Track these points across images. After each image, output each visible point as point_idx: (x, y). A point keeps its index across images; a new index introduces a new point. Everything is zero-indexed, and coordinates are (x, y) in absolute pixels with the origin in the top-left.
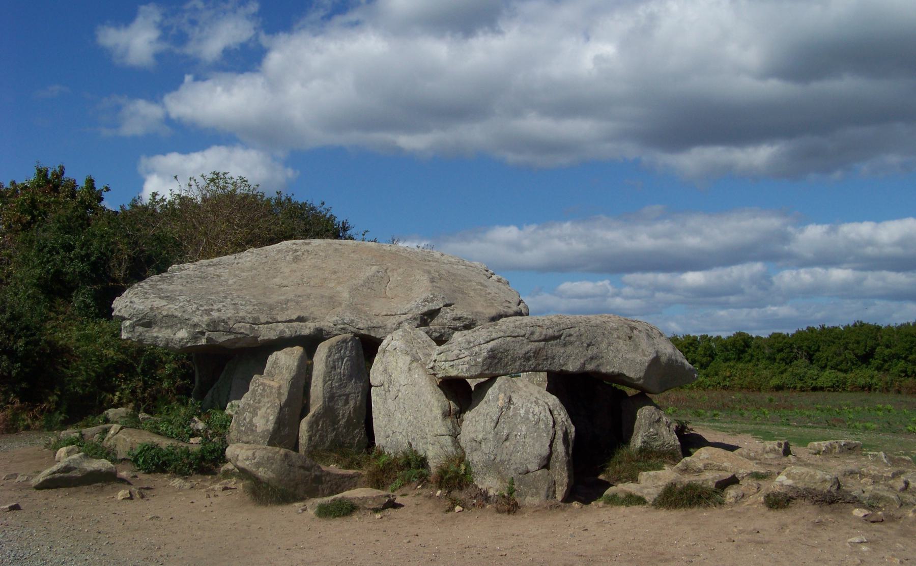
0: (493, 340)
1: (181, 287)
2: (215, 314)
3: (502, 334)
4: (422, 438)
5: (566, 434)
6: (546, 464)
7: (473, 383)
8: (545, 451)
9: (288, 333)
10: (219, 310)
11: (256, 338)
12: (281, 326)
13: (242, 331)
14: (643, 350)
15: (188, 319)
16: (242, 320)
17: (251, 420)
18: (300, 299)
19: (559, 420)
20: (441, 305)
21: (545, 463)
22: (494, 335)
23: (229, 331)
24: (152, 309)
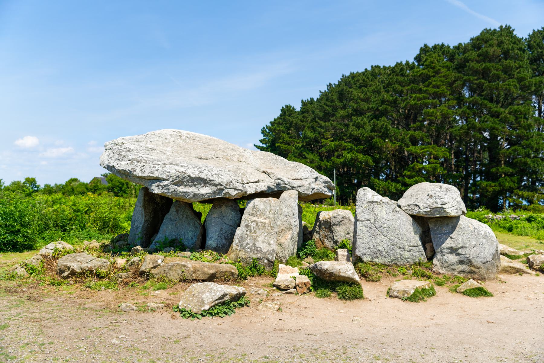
4: (400, 248)
11: (246, 192)
12: (254, 185)
13: (240, 188)
15: (213, 181)
17: (254, 244)
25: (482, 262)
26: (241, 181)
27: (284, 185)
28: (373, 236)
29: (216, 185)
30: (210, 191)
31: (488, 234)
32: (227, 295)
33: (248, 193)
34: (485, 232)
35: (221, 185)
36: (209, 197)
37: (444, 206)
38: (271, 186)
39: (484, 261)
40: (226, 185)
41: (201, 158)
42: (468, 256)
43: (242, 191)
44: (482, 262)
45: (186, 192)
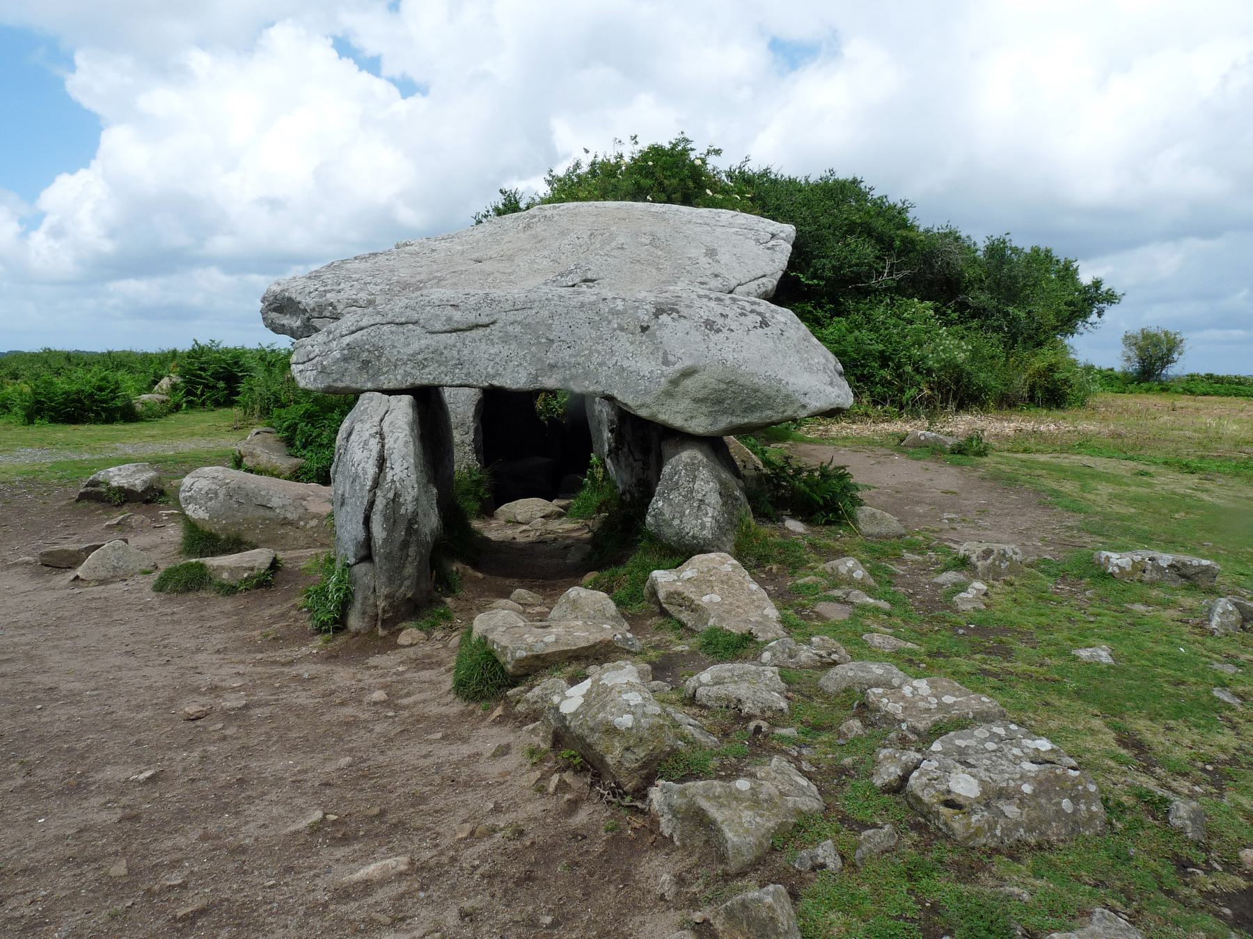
0: (362, 329)
3: (378, 319)
14: (665, 353)
21: (363, 553)
22: (363, 324)
40: (313, 310)
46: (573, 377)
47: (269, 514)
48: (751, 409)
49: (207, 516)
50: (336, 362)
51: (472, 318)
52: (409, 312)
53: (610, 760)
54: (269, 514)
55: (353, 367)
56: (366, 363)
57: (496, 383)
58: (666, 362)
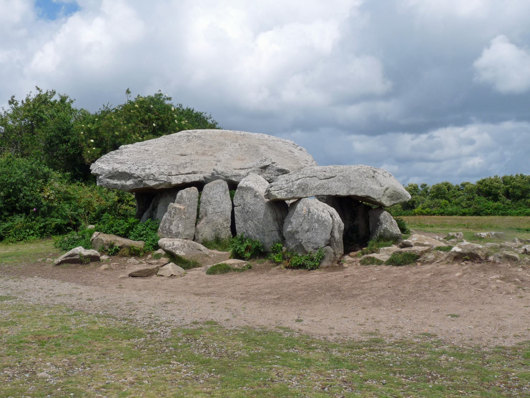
1: (127, 157)
2: (147, 171)
3: (304, 176)
5: (339, 227)
6: (329, 243)
7: (289, 202)
8: (328, 237)
9: (188, 181)
10: (150, 169)
11: (170, 183)
13: (163, 179)
15: (134, 174)
16: (162, 174)
17: (169, 227)
18: (193, 162)
19: (335, 220)
20: (270, 163)
22: (300, 177)
23: (156, 180)
24: (113, 169)
25: (313, 247)
26: (167, 174)
27: (217, 175)
28: (245, 221)
29: (135, 178)
30: (132, 183)
31: (320, 218)
32: (77, 254)
33: (173, 183)
34: (318, 216)
35: (140, 178)
36: (133, 187)
37: (271, 189)
38: (207, 177)
39: (316, 246)
41: (182, 155)
42: (300, 241)
43: (165, 182)
44: (313, 247)
45: (116, 184)
46: (358, 191)
47: (201, 252)
48: (398, 199)
49: (184, 254)
50: (296, 189)
51: (331, 175)
52: (313, 174)
53: (479, 254)
54: (201, 252)
55: (300, 190)
56: (303, 189)
57: (338, 194)
58: (381, 186)
